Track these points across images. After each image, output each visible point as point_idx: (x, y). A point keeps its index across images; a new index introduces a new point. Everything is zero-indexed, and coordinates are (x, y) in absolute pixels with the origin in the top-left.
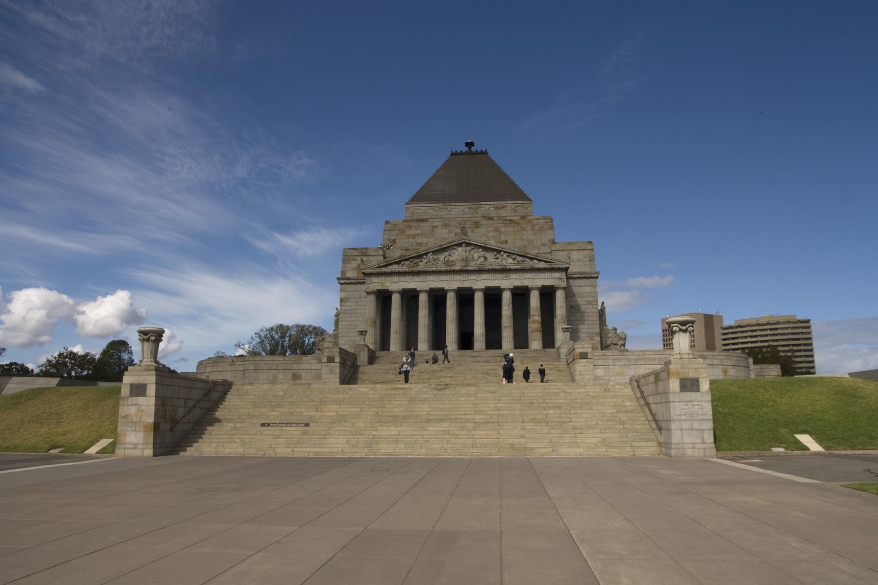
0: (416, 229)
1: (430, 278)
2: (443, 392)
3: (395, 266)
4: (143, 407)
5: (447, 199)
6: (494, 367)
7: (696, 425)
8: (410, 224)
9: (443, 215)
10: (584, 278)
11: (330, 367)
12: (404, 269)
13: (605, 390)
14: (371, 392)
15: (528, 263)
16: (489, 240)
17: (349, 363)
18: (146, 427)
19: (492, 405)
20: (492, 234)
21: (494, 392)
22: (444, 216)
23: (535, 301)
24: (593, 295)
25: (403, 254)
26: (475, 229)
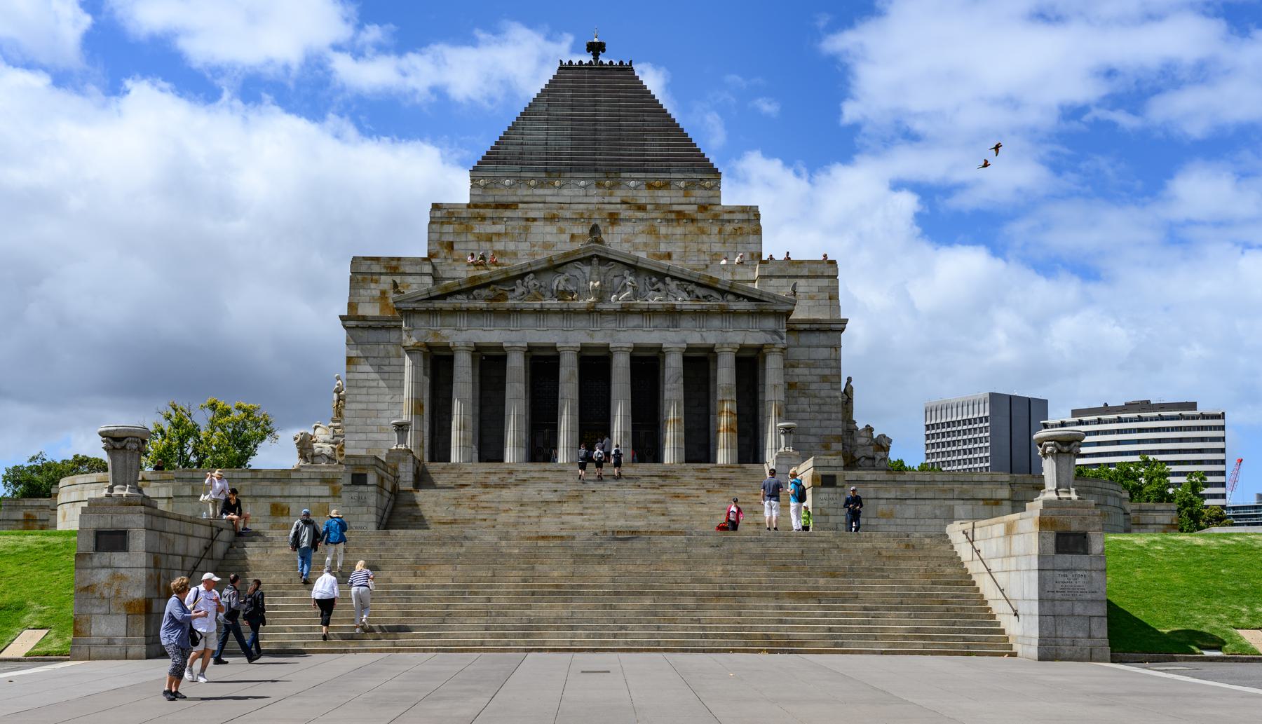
0: (494, 223)
1: (530, 321)
2: (629, 544)
3: (459, 297)
4: (122, 571)
6: (656, 497)
7: (1079, 609)
8: (482, 211)
9: (545, 195)
10: (818, 330)
11: (355, 495)
12: (478, 305)
13: (907, 546)
14: (504, 543)
15: (716, 302)
16: (636, 249)
17: (388, 486)
18: (130, 607)
19: (720, 568)
20: (641, 239)
21: (717, 546)
22: (549, 199)
23: (725, 375)
24: (833, 363)
25: (480, 278)
26: (610, 228)
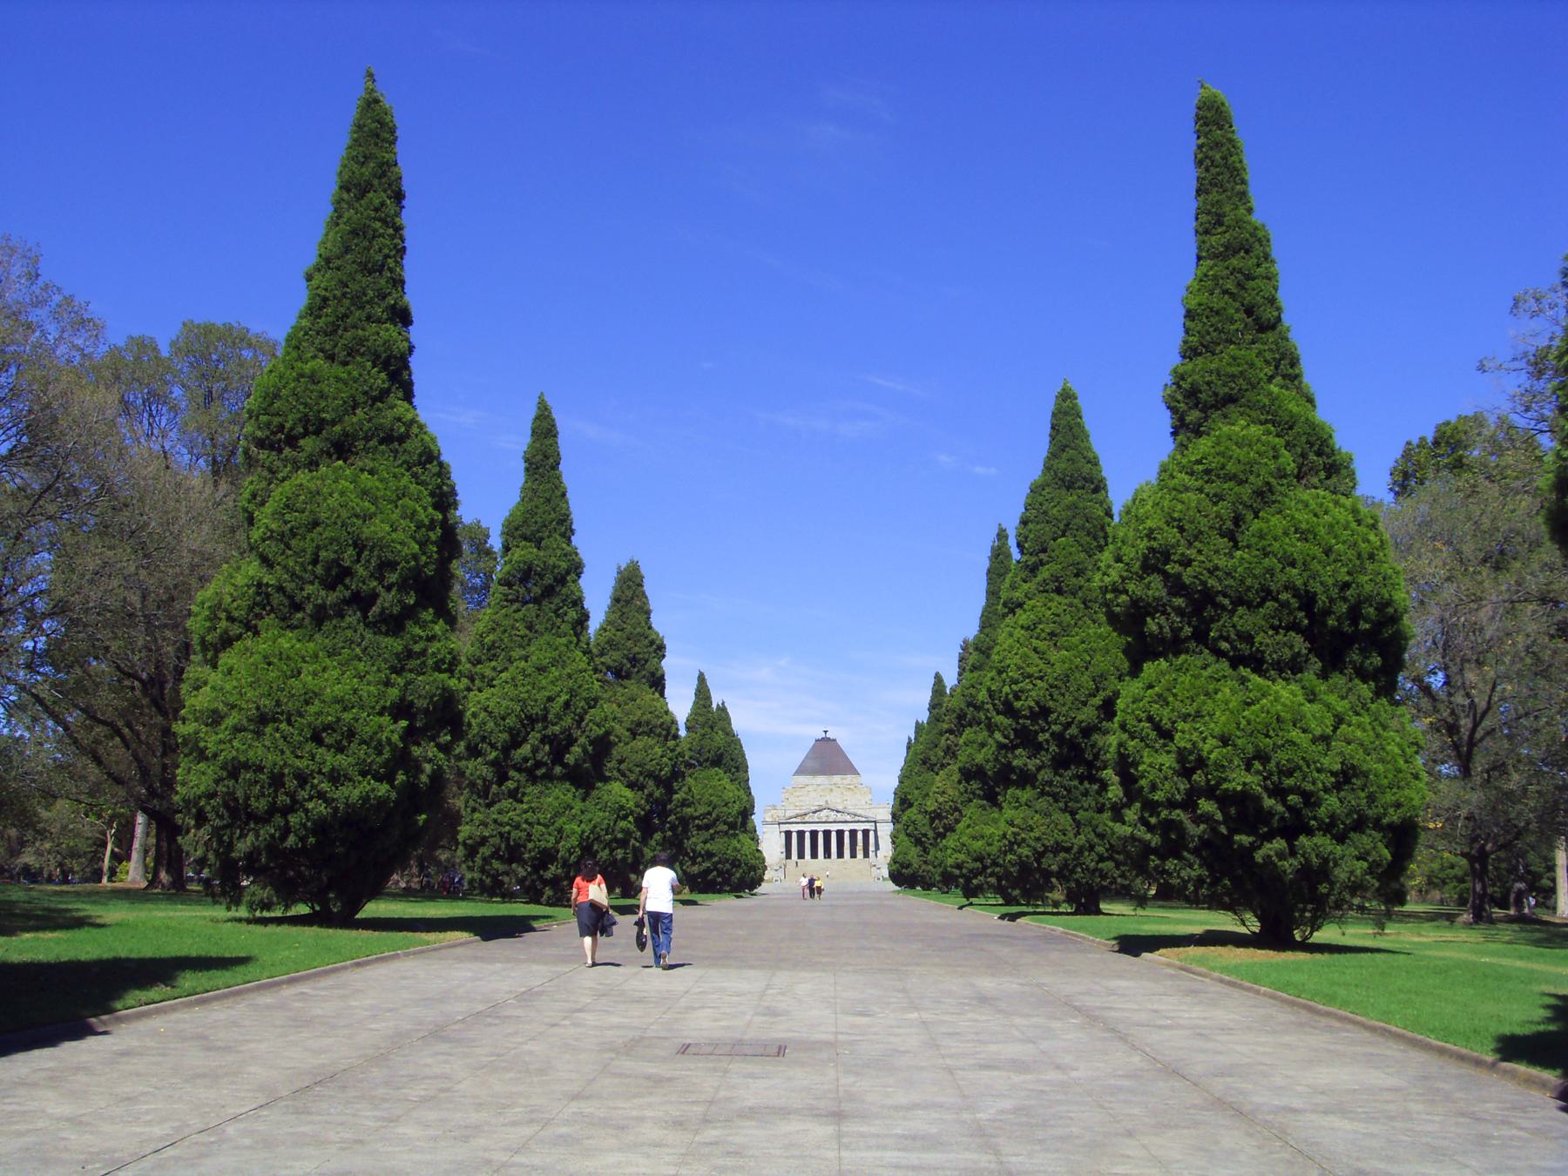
23: (860, 836)
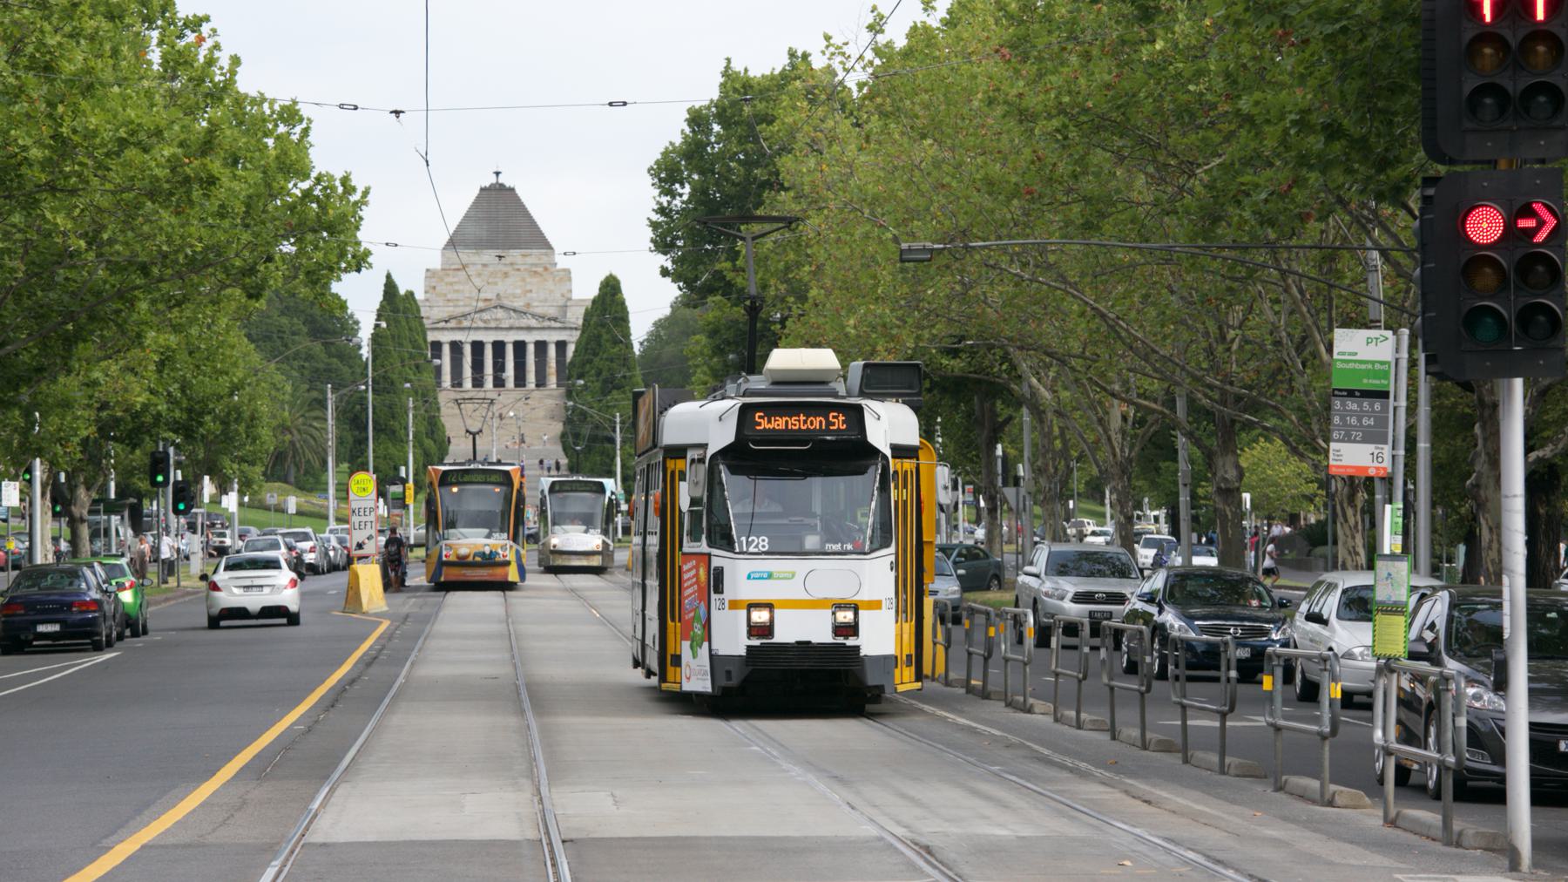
5: (480, 245)
15: (547, 324)
